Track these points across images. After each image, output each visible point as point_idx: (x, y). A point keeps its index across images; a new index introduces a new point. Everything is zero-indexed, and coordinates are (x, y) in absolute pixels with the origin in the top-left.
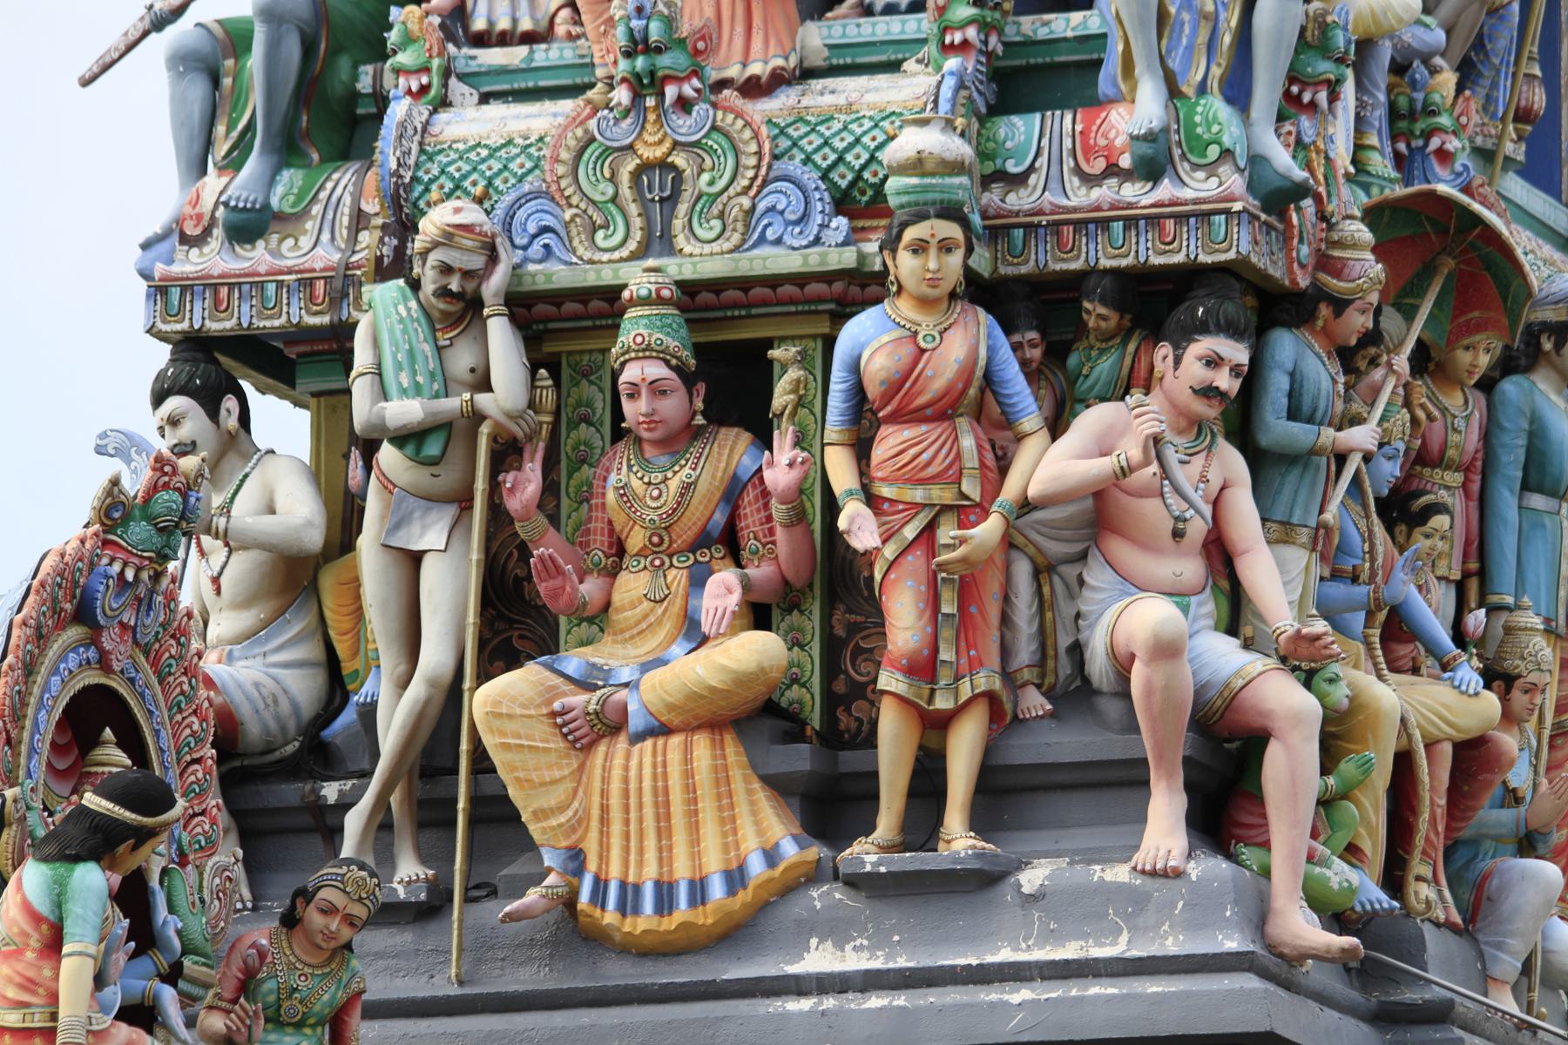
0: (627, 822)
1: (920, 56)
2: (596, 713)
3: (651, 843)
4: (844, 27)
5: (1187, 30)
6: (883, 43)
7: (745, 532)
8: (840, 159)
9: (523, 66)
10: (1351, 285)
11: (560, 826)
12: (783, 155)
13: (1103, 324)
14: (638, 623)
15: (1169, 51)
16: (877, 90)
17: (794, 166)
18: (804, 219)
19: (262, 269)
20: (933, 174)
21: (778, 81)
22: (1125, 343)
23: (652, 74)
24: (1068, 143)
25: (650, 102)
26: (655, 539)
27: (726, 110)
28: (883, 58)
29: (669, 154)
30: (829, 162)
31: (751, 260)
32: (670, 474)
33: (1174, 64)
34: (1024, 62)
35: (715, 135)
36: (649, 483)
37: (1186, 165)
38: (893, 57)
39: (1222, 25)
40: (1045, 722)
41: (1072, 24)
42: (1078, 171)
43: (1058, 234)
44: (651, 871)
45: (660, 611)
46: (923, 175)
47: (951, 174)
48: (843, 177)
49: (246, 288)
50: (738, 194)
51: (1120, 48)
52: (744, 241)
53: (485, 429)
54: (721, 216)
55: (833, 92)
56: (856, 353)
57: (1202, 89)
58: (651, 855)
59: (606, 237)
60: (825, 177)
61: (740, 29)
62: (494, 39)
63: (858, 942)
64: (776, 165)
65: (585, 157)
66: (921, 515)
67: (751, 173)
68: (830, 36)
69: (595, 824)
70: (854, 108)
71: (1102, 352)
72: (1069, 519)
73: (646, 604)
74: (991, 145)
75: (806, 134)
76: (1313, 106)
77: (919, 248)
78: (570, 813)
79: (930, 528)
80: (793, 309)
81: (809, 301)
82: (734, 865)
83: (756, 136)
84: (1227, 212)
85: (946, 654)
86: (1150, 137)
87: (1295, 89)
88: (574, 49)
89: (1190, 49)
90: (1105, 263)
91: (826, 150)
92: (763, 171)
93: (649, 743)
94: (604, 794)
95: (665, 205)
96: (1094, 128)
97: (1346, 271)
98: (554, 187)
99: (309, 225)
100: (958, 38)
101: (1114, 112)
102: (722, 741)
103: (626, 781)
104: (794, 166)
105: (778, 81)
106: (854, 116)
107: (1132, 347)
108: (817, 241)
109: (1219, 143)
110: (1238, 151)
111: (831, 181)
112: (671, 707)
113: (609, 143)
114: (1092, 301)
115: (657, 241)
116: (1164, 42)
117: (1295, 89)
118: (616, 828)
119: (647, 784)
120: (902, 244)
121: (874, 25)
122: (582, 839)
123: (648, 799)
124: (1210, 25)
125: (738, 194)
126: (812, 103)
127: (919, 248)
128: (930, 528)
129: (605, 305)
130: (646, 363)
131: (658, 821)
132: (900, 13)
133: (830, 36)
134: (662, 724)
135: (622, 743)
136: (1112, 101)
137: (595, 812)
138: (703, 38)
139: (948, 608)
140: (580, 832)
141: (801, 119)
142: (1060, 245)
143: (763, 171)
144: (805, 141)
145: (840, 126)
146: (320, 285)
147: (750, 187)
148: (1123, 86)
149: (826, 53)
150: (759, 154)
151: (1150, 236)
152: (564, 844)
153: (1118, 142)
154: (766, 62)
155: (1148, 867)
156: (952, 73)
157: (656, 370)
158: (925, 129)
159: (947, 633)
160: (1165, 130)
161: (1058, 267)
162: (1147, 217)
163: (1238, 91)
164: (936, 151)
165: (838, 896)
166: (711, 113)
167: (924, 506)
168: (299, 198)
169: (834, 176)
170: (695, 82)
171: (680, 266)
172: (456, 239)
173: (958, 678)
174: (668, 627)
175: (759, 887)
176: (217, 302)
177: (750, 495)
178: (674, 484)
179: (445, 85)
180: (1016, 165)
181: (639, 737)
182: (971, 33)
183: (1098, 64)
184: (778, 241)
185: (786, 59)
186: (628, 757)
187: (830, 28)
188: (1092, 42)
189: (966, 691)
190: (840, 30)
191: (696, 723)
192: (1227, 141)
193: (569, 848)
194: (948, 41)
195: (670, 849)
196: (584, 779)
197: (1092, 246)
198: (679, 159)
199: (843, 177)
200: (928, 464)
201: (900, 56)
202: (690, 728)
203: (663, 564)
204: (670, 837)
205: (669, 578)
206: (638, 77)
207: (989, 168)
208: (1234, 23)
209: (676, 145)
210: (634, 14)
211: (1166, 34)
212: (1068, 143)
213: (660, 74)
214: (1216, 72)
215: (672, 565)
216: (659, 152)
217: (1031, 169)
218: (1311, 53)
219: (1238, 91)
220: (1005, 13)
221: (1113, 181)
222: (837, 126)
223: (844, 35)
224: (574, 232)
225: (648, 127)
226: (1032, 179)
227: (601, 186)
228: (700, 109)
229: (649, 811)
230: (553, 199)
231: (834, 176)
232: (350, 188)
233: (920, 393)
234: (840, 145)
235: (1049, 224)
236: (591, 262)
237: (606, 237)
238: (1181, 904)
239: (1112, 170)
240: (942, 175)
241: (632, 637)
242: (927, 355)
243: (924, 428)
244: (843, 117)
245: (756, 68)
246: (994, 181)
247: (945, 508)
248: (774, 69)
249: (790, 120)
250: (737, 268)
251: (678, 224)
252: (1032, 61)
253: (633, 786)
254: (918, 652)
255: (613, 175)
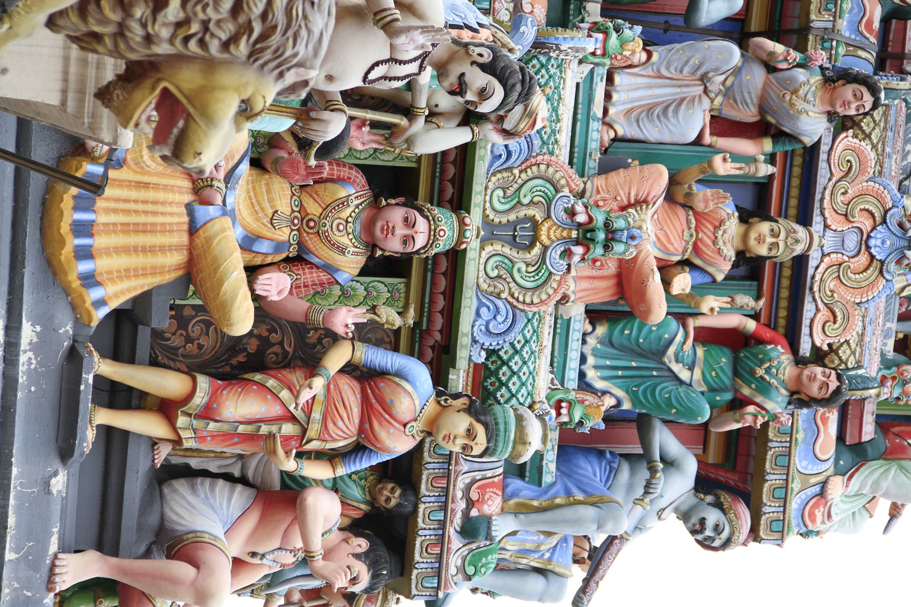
0: (136, 201)
2: (211, 186)
7: (301, 272)
9: (592, 114)
11: (142, 157)
13: (383, 498)
14: (259, 204)
20: (514, 447)
22: (365, 503)
23: (592, 240)
26: (312, 224)
31: (471, 298)
32: (351, 236)
35: (546, 274)
36: (347, 222)
37: (465, 553)
40: (150, 463)
41: (550, 464)
42: (474, 482)
44: (102, 219)
45: (264, 221)
46: (515, 442)
50: (510, 289)
52: (482, 291)
53: (403, 121)
54: (499, 277)
56: (410, 378)
59: (498, 196)
62: (609, 88)
63: (34, 361)
65: (548, 185)
66: (303, 415)
68: (575, 321)
71: (363, 488)
72: (270, 473)
73: (270, 212)
77: (470, 433)
79: (293, 419)
80: (427, 301)
82: (99, 279)
85: (212, 426)
88: (595, 149)
90: (422, 507)
92: (521, 306)
93: (186, 219)
94: (156, 187)
96: (495, 490)
98: (533, 161)
103: (163, 203)
107: (363, 506)
108: (475, 341)
112: (209, 240)
114: (400, 496)
118: (133, 194)
119: (160, 219)
120: (474, 423)
123: (150, 219)
125: (510, 289)
128: (293, 419)
129: (460, 203)
130: (426, 235)
131: (134, 224)
132: (580, 365)
133: (575, 321)
134: (197, 231)
135: (188, 198)
137: (146, 179)
138: (602, 265)
139: (241, 429)
140: (134, 167)
147: (512, 296)
149: (565, 317)
151: (433, 537)
152: (129, 157)
155: (57, 570)
159: (225, 427)
161: (424, 477)
162: (443, 535)
165: (66, 344)
167: (309, 418)
171: (475, 250)
172: (527, 119)
173: (195, 431)
174: (255, 226)
175: (81, 296)
177: (324, 277)
178: (345, 240)
181: (189, 207)
184: (478, 314)
186: (178, 204)
187: (580, 321)
188: (537, 475)
189: (184, 434)
190: (577, 328)
191: (195, 253)
193: (125, 160)
195: (115, 232)
197: (433, 499)
198: (537, 250)
200: (335, 424)
203: (294, 225)
205: (285, 229)
206: (593, 230)
209: (545, 248)
213: (592, 246)
215: (292, 230)
216: (544, 238)
224: (505, 174)
229: (141, 219)
230: (526, 160)
233: (380, 424)
236: (486, 188)
237: (498, 196)
238: (29, 594)
239: (470, 504)
241: (250, 198)
242: (402, 428)
243: (357, 421)
247: (304, 431)
250: (468, 288)
251: (498, 247)
253: (160, 208)
254: (220, 415)
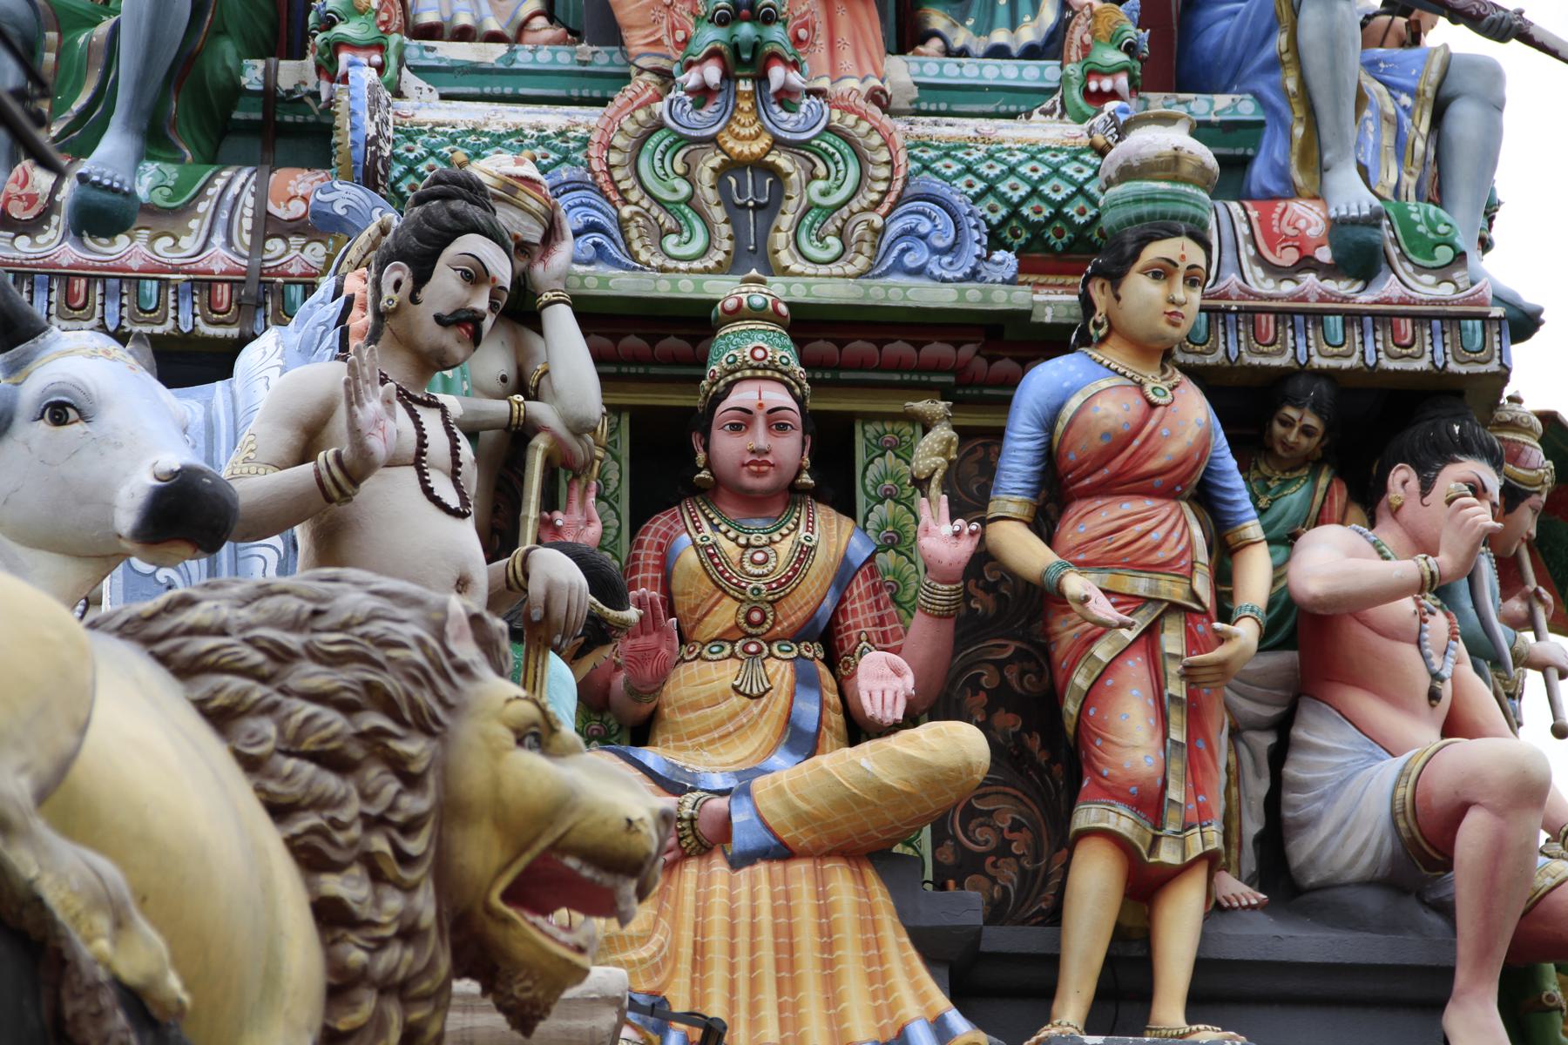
0: (732, 968)
2: (692, 819)
3: (768, 997)
6: (993, 88)
9: (501, 66)
10: (1533, 474)
11: (642, 961)
13: (1304, 441)
18: (953, 249)
19: (135, 264)
20: (1186, 181)
22: (1314, 476)
24: (1243, 229)
26: (756, 616)
29: (768, 153)
31: (887, 288)
32: (776, 537)
35: (830, 137)
36: (747, 546)
42: (1260, 259)
43: (1255, 324)
45: (756, 710)
46: (1175, 180)
49: (110, 282)
50: (864, 210)
53: (540, 443)
54: (840, 233)
56: (1054, 402)
58: (769, 1013)
59: (678, 245)
62: (447, 34)
65: (650, 144)
66: (1143, 613)
68: (922, 74)
69: (685, 966)
71: (1285, 483)
73: (737, 701)
77: (1163, 271)
78: (652, 947)
80: (897, 377)
81: (922, 368)
84: (1484, 318)
88: (572, 54)
90: (1318, 362)
92: (898, 186)
93: (761, 868)
94: (700, 929)
95: (759, 213)
97: (1524, 457)
98: (602, 178)
99: (194, 224)
102: (862, 874)
103: (732, 914)
107: (1323, 482)
108: (974, 275)
109: (1452, 246)
112: (801, 819)
113: (684, 131)
115: (750, 255)
119: (765, 918)
120: (1139, 265)
122: (665, 985)
123: (766, 938)
125: (864, 210)
127: (1163, 271)
128: (1151, 634)
129: (696, 322)
130: (765, 385)
132: (1010, 57)
134: (783, 844)
137: (686, 951)
138: (805, 25)
139: (1178, 734)
140: (664, 975)
142: (1256, 335)
146: (223, 292)
149: (915, 94)
151: (1379, 336)
157: (777, 396)
159: (1176, 766)
161: (1256, 361)
168: (177, 191)
171: (788, 285)
172: (520, 195)
173: (1187, 827)
174: (767, 730)
176: (69, 297)
177: (860, 587)
178: (785, 548)
179: (399, 73)
181: (740, 861)
184: (919, 272)
186: (732, 885)
187: (921, 64)
188: (1241, 132)
189: (1196, 847)
196: (668, 906)
197: (1301, 341)
198: (782, 160)
200: (1157, 547)
202: (819, 853)
203: (760, 650)
204: (794, 991)
206: (736, 48)
209: (778, 143)
213: (768, 49)
215: (771, 655)
216: (756, 147)
223: (941, 74)
224: (633, 233)
229: (767, 955)
230: (602, 192)
232: (250, 187)
233: (1151, 456)
235: (1239, 311)
236: (663, 269)
237: (678, 245)
239: (1307, 263)
241: (711, 742)
242: (1159, 411)
243: (1149, 503)
247: (1174, 608)
250: (866, 295)
251: (780, 239)
253: (743, 920)
254: (1151, 778)
255: (688, 171)
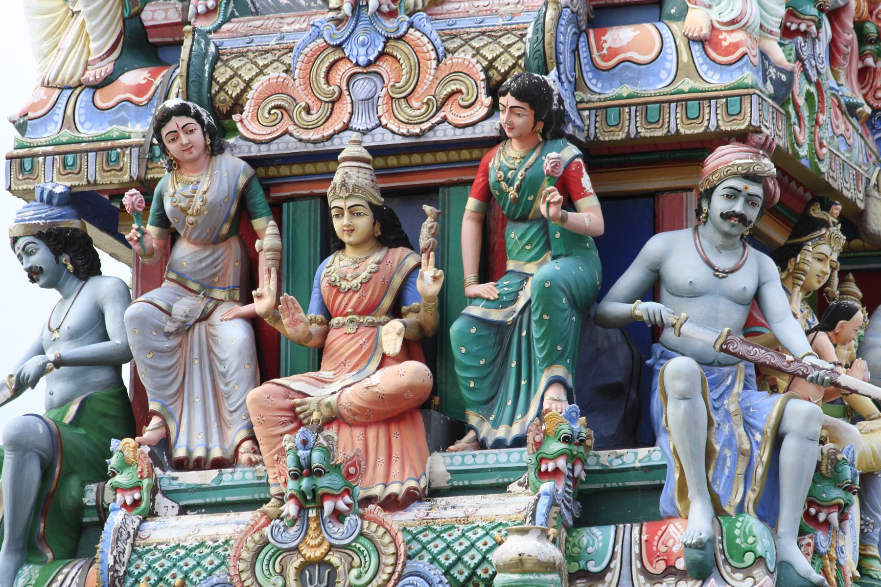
1: (522, 480)
4: (463, 457)
5: (729, 464)
8: (459, 559)
12: (415, 555)
15: (714, 479)
16: (488, 506)
17: (422, 564)
20: (531, 572)
21: (411, 498)
23: (314, 492)
25: (312, 514)
27: (371, 520)
28: (493, 481)
29: (326, 554)
30: (450, 561)
33: (719, 489)
34: (602, 486)
35: (362, 540)
37: (728, 569)
38: (501, 481)
39: (756, 459)
42: (644, 571)
46: (524, 572)
47: (544, 573)
48: (461, 573)
51: (677, 476)
55: (454, 507)
57: (741, 509)
60: (447, 573)
61: (382, 457)
64: (410, 563)
67: (389, 570)
68: (452, 464)
70: (470, 520)
74: (576, 550)
75: (433, 540)
76: (827, 523)
83: (394, 541)
86: (700, 546)
87: (813, 511)
89: (731, 477)
91: (449, 552)
92: (399, 568)
96: (657, 538)
100: (551, 466)
101: (671, 526)
104: (422, 564)
105: (411, 498)
106: (470, 526)
110: (768, 558)
111: (452, 576)
113: (280, 546)
116: (711, 472)
117: (813, 511)
121: (486, 455)
124: (747, 459)
126: (437, 515)
133: (452, 464)
136: (670, 517)
138: (353, 465)
141: (429, 528)
143: (399, 568)
144: (432, 545)
145: (459, 533)
148: (678, 506)
149: (449, 477)
150: (396, 554)
153: (675, 549)
154: (402, 484)
156: (546, 494)
158: (526, 537)
160: (712, 540)
163: (768, 511)
164: (533, 554)
166: (359, 522)
169: (454, 572)
170: (347, 499)
180: (595, 566)
182: (561, 463)
183: (660, 488)
185: (418, 481)
188: (655, 471)
190: (460, 459)
192: (760, 550)
194: (543, 469)
198: (334, 559)
199: (461, 573)
201: (506, 480)
206: (303, 494)
207: (575, 567)
208: (765, 459)
210: (300, 445)
211: (712, 466)
212: (636, 549)
213: (320, 492)
214: (752, 496)
216: (319, 552)
217: (608, 569)
218: (826, 483)
219: (768, 511)
220: (588, 448)
221: (671, 580)
222: (456, 533)
223: (463, 463)
225: (310, 532)
226: (609, 577)
227: (273, 579)
228: (351, 519)
231: (454, 572)
234: (459, 549)
240: (538, 573)
244: (461, 527)
245: (394, 488)
246: (578, 578)
248: (409, 489)
249: (421, 528)
252: (608, 485)
